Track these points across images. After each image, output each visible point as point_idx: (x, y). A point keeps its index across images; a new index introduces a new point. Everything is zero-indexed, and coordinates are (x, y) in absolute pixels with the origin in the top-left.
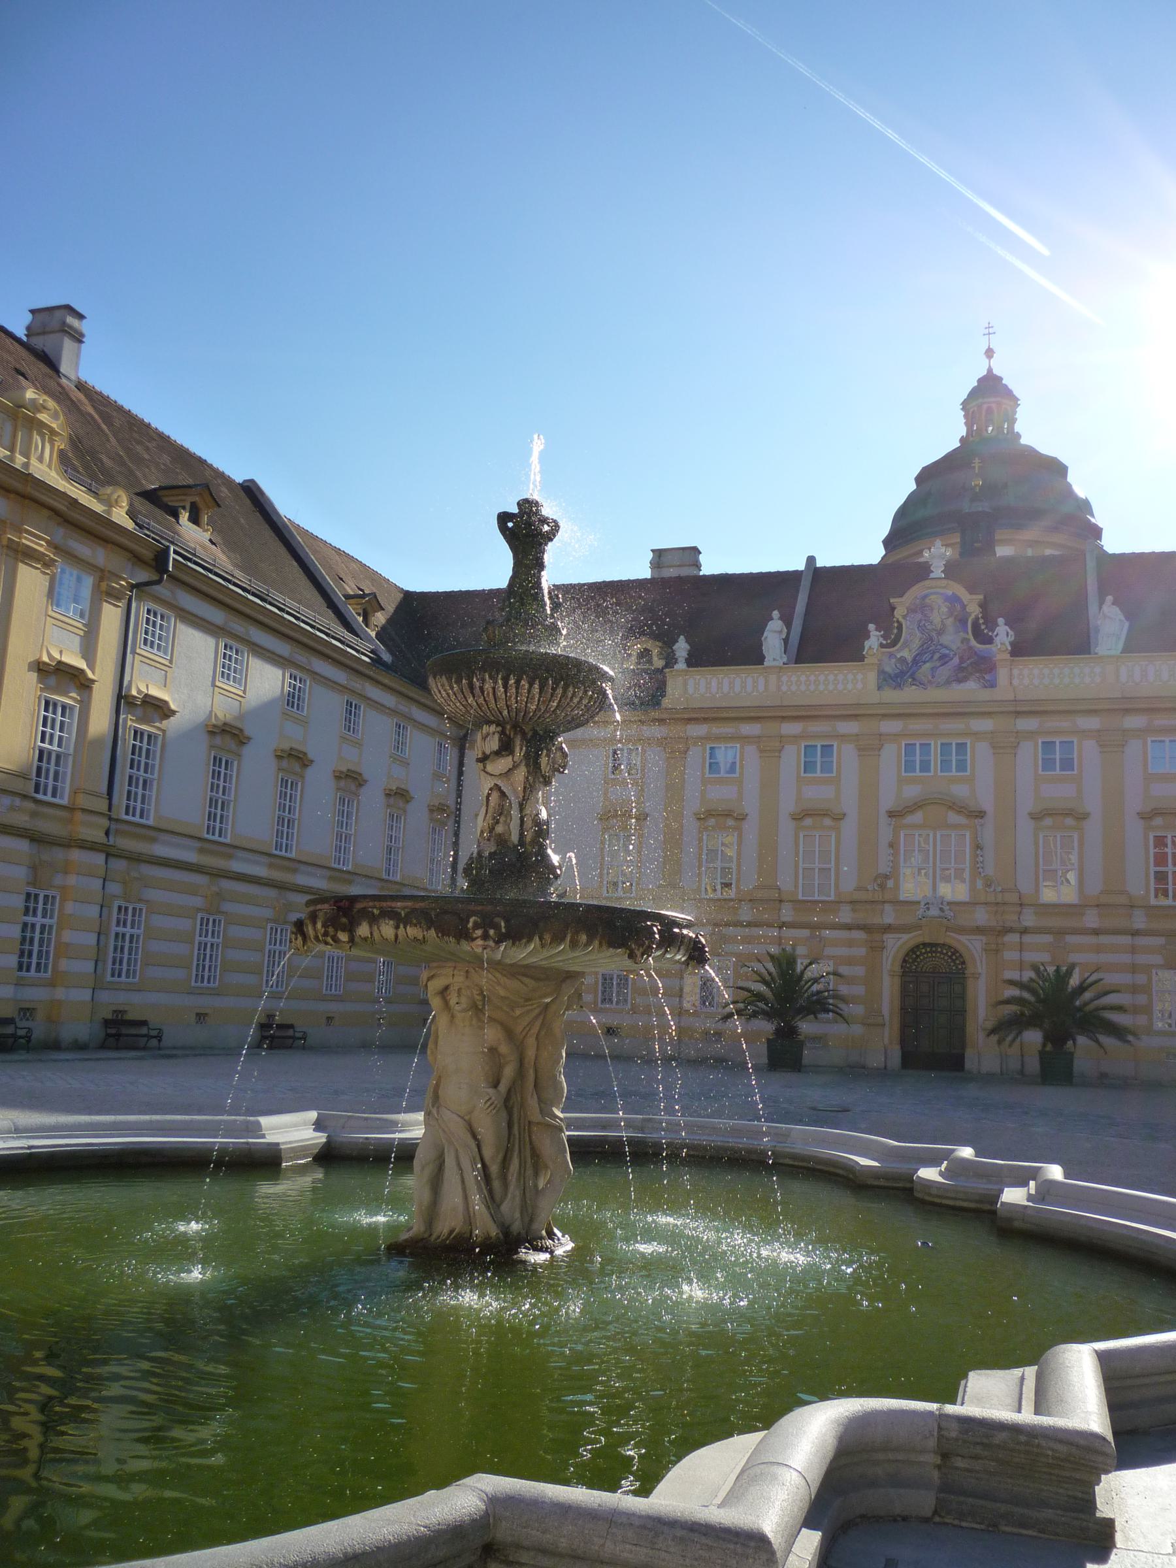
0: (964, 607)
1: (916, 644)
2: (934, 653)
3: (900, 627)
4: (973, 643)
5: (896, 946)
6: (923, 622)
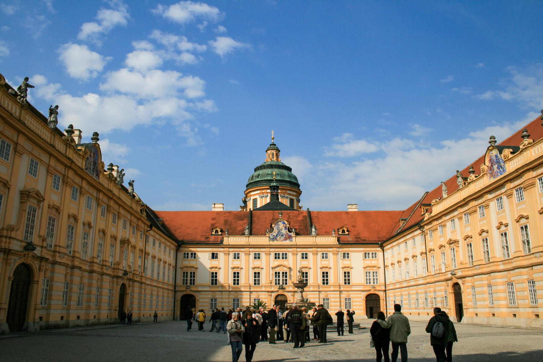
0: (286, 225)
1: (276, 232)
3: (273, 228)
4: (288, 232)
5: (274, 295)
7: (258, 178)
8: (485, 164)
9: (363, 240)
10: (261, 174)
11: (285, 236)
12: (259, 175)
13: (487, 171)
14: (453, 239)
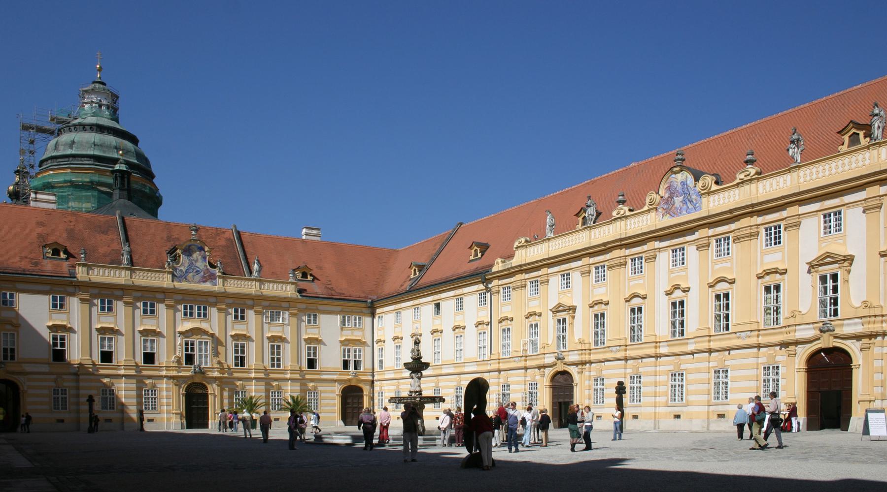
1: (187, 265)
2: (194, 269)
4: (209, 267)
7: (72, 149)
8: (657, 193)
9: (341, 294)
12: (73, 142)
13: (659, 204)
14: (567, 302)
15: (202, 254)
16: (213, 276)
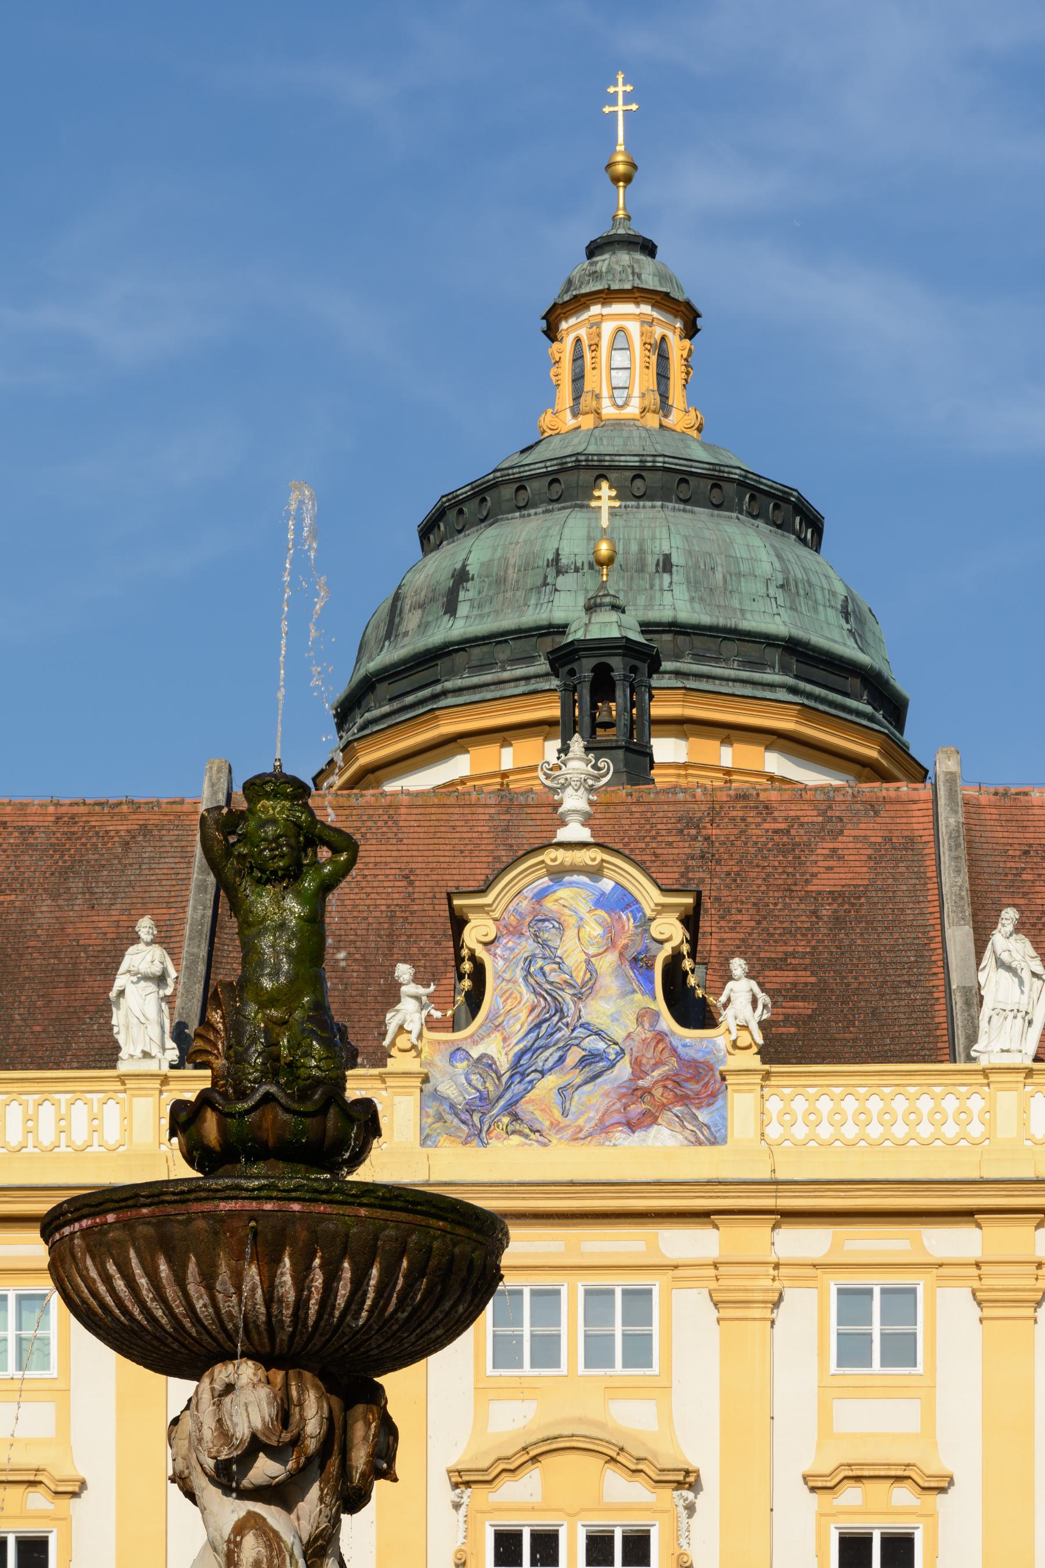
1: (519, 1023)
2: (567, 1047)
4: (667, 1022)
6: (540, 963)
7: (451, 608)
10: (487, 565)
11: (624, 1070)
12: (461, 577)
15: (624, 942)
16: (696, 1078)
